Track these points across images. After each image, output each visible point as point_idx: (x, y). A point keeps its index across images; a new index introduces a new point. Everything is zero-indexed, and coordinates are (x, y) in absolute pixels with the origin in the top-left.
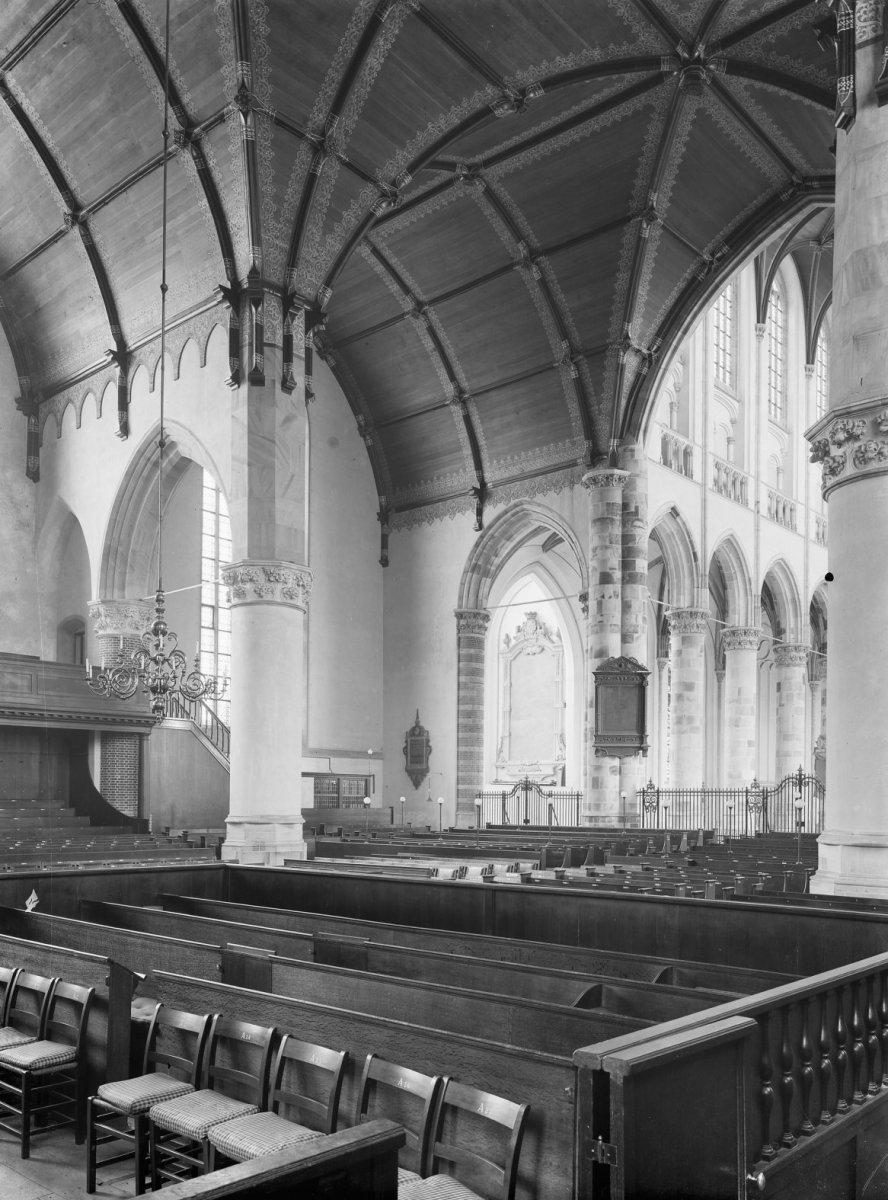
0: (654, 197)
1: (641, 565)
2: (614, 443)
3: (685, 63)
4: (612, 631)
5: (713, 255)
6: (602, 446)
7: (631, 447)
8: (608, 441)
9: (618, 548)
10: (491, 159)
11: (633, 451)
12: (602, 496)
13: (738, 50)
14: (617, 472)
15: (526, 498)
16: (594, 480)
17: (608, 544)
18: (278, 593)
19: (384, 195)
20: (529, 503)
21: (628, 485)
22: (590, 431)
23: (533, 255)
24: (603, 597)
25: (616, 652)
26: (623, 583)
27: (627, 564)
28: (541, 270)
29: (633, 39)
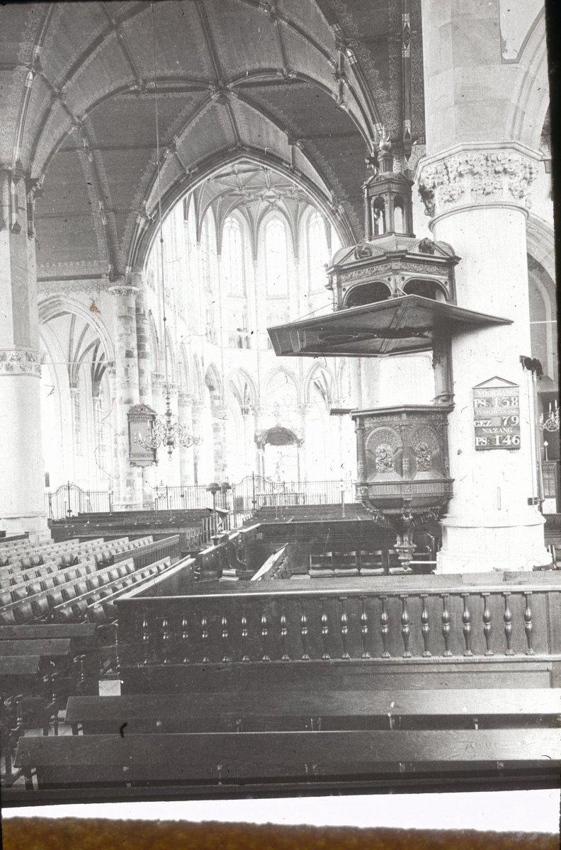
0: (176, 138)
1: (148, 347)
2: (128, 269)
3: (221, 88)
4: (135, 388)
5: (190, 170)
6: (120, 268)
7: (139, 273)
8: (125, 268)
9: (135, 335)
10: (99, 100)
11: (140, 276)
12: (125, 303)
13: (252, 92)
14: (134, 288)
15: (63, 294)
16: (119, 291)
17: (129, 332)
18: (33, 369)
19: (74, 123)
20: (65, 297)
21: (139, 296)
22: (113, 259)
23: (91, 148)
24: (128, 366)
25: (136, 402)
26: (139, 358)
27: (140, 347)
28: (94, 156)
29: (202, 70)
